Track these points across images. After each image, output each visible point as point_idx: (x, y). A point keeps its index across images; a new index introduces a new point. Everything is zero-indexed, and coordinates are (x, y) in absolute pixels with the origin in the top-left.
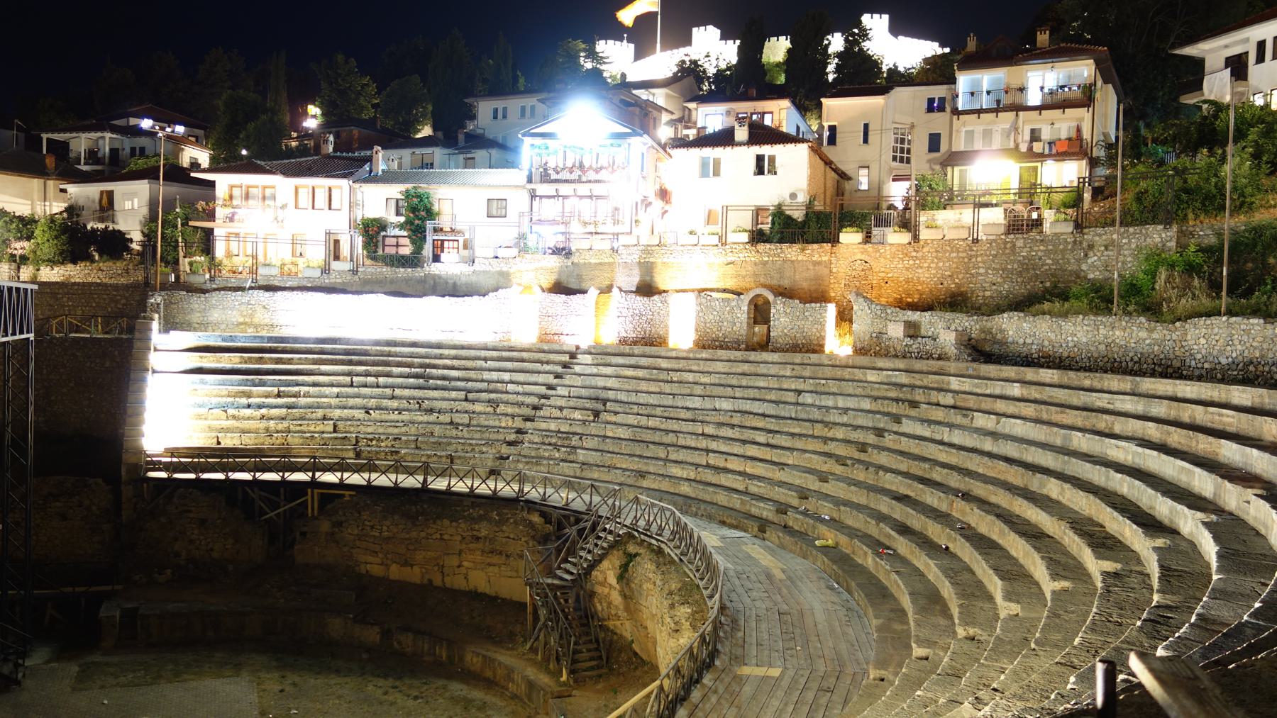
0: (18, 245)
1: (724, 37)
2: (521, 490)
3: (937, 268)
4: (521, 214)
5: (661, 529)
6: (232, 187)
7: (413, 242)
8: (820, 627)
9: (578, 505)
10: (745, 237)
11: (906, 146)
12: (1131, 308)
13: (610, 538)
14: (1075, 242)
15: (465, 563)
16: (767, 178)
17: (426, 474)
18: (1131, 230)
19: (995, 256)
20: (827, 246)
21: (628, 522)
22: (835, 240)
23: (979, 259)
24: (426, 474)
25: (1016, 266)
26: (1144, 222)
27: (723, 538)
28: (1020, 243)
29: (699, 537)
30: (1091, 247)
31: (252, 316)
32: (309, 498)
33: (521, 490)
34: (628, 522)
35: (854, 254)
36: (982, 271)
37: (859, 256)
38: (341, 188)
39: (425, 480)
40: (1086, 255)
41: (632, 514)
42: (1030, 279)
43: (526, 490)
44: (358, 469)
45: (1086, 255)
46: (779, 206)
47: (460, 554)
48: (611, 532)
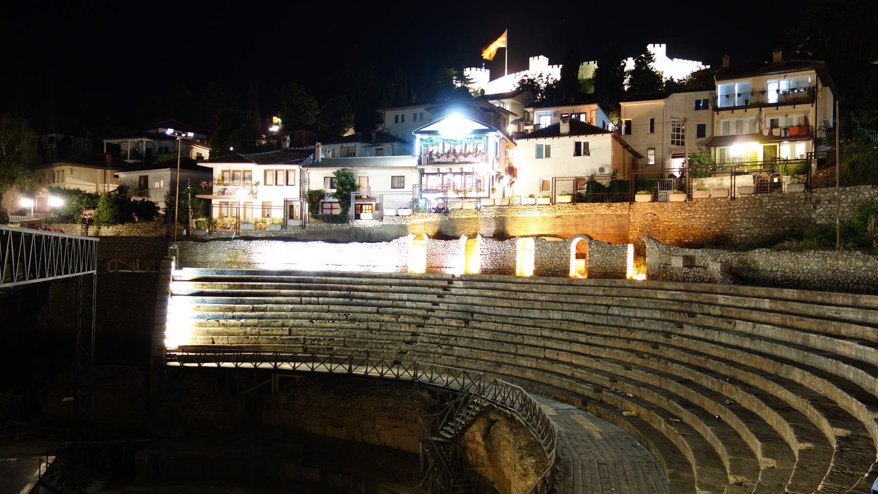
0: (87, 212)
2: (415, 375)
3: (706, 218)
4: (414, 186)
5: (513, 402)
6: (223, 172)
7: (342, 206)
8: (628, 474)
9: (455, 385)
10: (568, 199)
13: (477, 409)
14: (806, 198)
15: (377, 426)
16: (583, 158)
17: (351, 364)
18: (848, 189)
19: (748, 209)
20: (627, 204)
21: (490, 398)
22: (632, 200)
23: (736, 211)
24: (351, 364)
26: (856, 183)
27: (557, 409)
28: (765, 200)
29: (540, 409)
30: (818, 201)
31: (235, 257)
32: (273, 380)
33: (415, 375)
34: (490, 398)
35: (646, 209)
36: (738, 219)
37: (649, 211)
38: (294, 170)
39: (350, 368)
40: (815, 207)
41: (493, 392)
42: (774, 225)
43: (419, 375)
45: (815, 207)
46: (592, 177)
47: (374, 419)
48: (477, 405)
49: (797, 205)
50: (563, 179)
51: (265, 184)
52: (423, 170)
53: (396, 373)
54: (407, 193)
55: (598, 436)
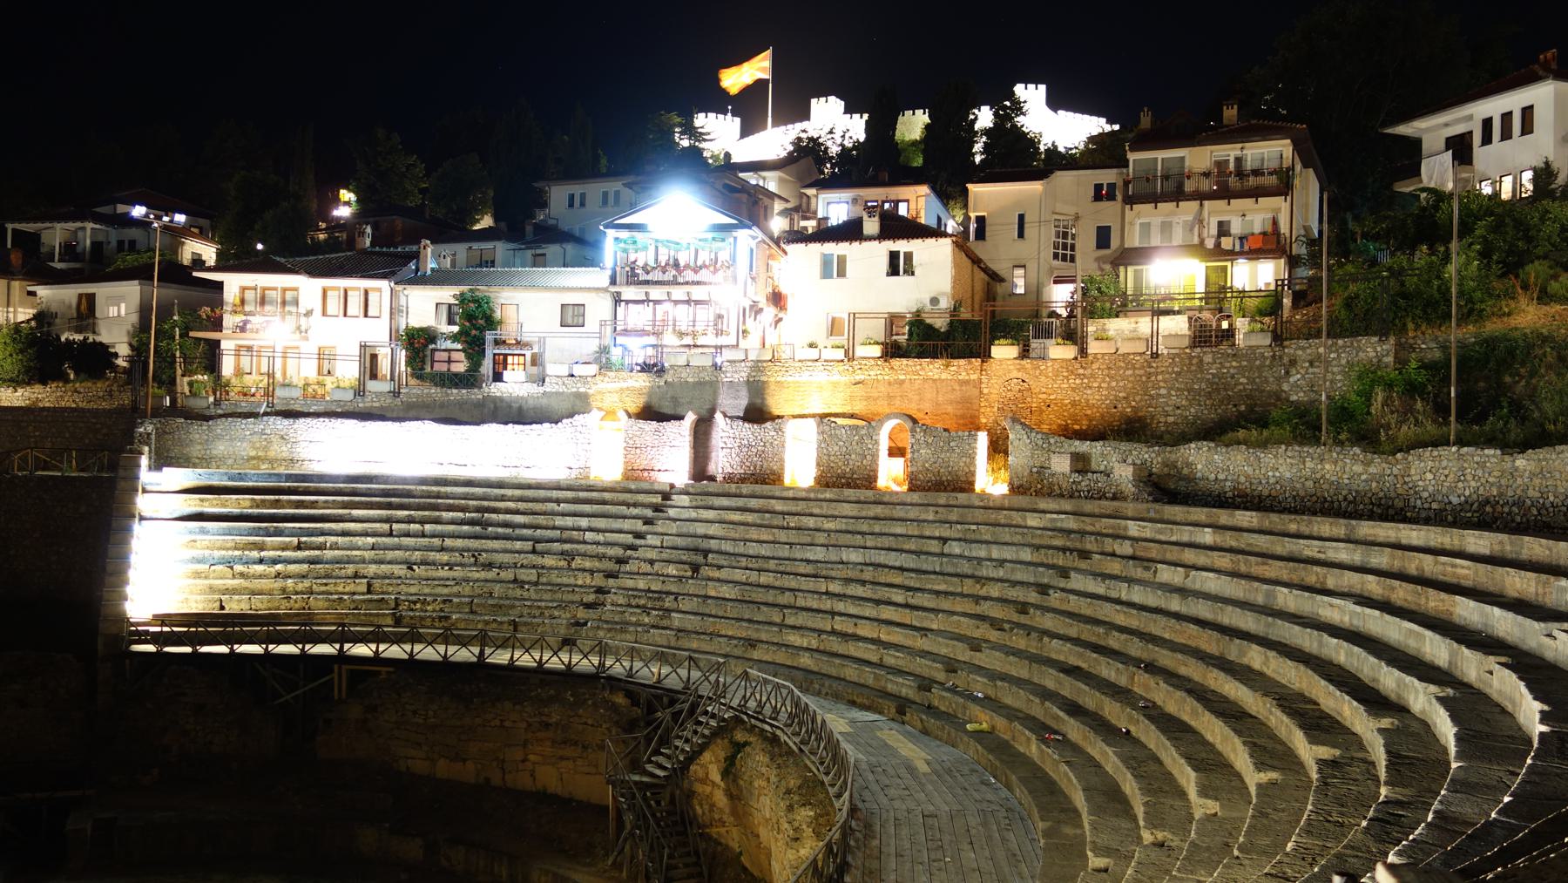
1: (849, 110)
2: (602, 664)
3: (1109, 388)
4: (603, 324)
5: (776, 711)
6: (243, 289)
7: (469, 357)
8: (973, 832)
9: (673, 682)
10: (876, 351)
11: (1069, 241)
12: (1343, 437)
13: (713, 723)
14: (1274, 357)
15: (532, 757)
16: (902, 280)
18: (1340, 342)
19: (1179, 374)
20: (976, 362)
21: (735, 703)
22: (985, 355)
25: (1203, 386)
26: (1354, 333)
27: (853, 722)
28: (1208, 358)
29: (823, 721)
30: (1293, 363)
31: (266, 449)
33: (602, 664)
34: (735, 703)
35: (1010, 371)
36: (1163, 391)
37: (1015, 374)
38: (379, 290)
39: (482, 652)
40: (1287, 373)
41: (741, 693)
42: (1221, 402)
43: (608, 663)
44: (397, 640)
45: (1287, 373)
46: (918, 313)
47: (525, 745)
48: (713, 716)
49: (1259, 368)
50: (868, 316)
51: (324, 314)
52: (619, 294)
53: (566, 660)
54: (589, 336)
55: (923, 767)
